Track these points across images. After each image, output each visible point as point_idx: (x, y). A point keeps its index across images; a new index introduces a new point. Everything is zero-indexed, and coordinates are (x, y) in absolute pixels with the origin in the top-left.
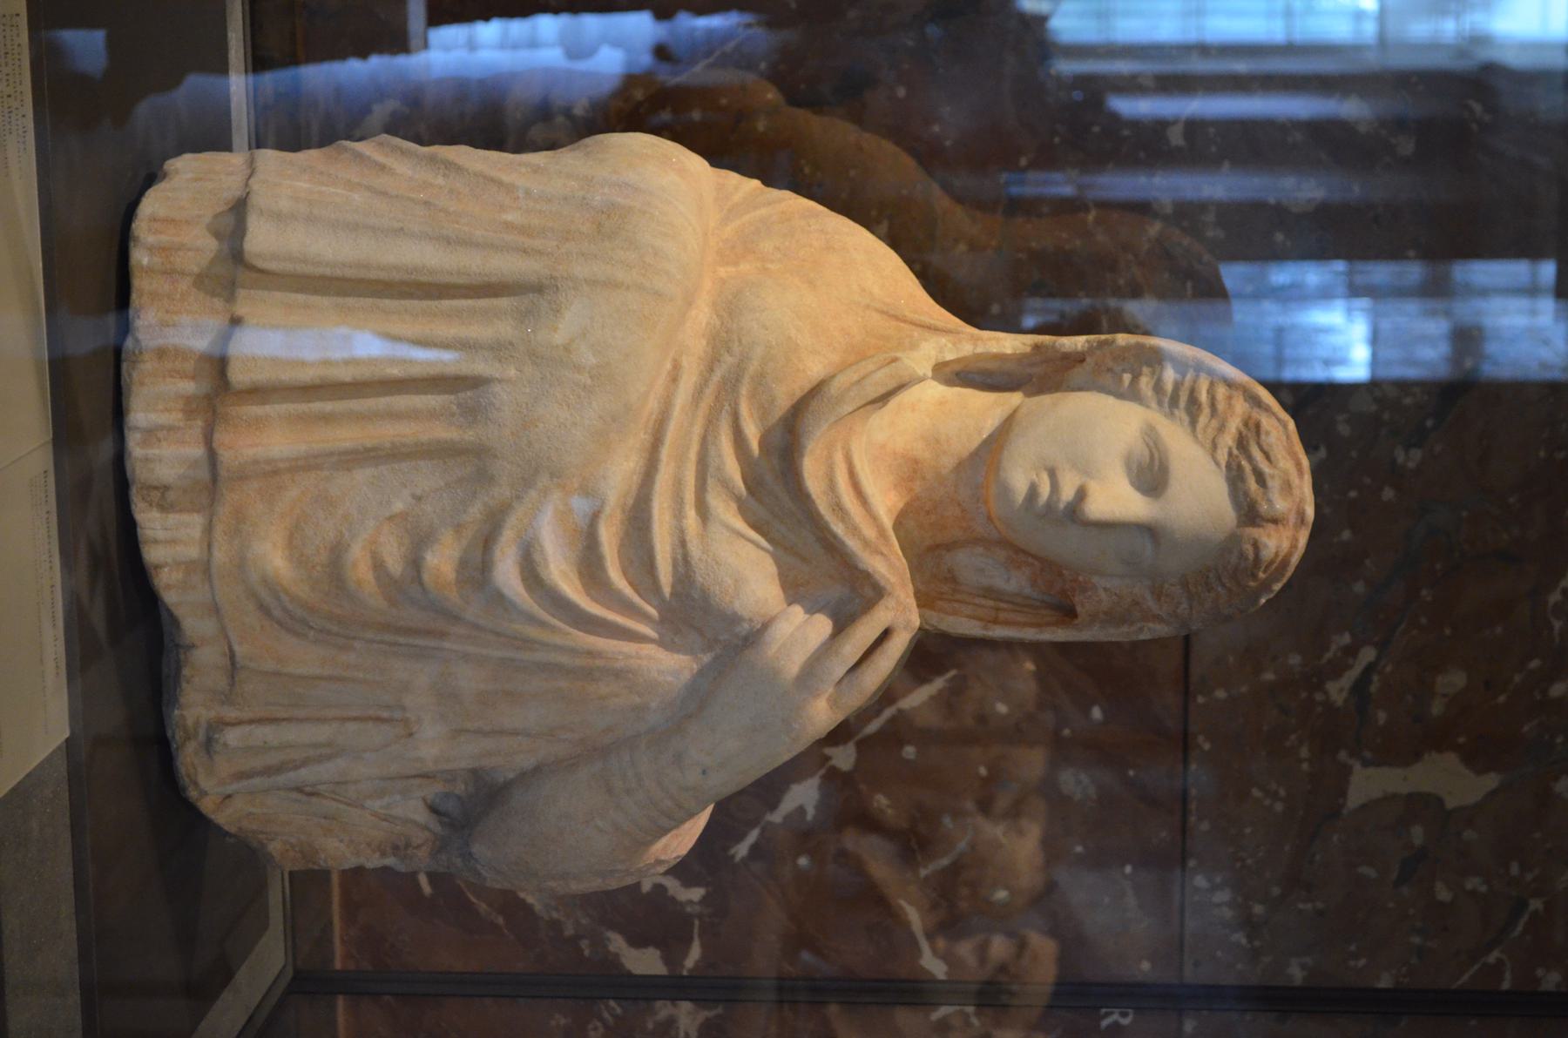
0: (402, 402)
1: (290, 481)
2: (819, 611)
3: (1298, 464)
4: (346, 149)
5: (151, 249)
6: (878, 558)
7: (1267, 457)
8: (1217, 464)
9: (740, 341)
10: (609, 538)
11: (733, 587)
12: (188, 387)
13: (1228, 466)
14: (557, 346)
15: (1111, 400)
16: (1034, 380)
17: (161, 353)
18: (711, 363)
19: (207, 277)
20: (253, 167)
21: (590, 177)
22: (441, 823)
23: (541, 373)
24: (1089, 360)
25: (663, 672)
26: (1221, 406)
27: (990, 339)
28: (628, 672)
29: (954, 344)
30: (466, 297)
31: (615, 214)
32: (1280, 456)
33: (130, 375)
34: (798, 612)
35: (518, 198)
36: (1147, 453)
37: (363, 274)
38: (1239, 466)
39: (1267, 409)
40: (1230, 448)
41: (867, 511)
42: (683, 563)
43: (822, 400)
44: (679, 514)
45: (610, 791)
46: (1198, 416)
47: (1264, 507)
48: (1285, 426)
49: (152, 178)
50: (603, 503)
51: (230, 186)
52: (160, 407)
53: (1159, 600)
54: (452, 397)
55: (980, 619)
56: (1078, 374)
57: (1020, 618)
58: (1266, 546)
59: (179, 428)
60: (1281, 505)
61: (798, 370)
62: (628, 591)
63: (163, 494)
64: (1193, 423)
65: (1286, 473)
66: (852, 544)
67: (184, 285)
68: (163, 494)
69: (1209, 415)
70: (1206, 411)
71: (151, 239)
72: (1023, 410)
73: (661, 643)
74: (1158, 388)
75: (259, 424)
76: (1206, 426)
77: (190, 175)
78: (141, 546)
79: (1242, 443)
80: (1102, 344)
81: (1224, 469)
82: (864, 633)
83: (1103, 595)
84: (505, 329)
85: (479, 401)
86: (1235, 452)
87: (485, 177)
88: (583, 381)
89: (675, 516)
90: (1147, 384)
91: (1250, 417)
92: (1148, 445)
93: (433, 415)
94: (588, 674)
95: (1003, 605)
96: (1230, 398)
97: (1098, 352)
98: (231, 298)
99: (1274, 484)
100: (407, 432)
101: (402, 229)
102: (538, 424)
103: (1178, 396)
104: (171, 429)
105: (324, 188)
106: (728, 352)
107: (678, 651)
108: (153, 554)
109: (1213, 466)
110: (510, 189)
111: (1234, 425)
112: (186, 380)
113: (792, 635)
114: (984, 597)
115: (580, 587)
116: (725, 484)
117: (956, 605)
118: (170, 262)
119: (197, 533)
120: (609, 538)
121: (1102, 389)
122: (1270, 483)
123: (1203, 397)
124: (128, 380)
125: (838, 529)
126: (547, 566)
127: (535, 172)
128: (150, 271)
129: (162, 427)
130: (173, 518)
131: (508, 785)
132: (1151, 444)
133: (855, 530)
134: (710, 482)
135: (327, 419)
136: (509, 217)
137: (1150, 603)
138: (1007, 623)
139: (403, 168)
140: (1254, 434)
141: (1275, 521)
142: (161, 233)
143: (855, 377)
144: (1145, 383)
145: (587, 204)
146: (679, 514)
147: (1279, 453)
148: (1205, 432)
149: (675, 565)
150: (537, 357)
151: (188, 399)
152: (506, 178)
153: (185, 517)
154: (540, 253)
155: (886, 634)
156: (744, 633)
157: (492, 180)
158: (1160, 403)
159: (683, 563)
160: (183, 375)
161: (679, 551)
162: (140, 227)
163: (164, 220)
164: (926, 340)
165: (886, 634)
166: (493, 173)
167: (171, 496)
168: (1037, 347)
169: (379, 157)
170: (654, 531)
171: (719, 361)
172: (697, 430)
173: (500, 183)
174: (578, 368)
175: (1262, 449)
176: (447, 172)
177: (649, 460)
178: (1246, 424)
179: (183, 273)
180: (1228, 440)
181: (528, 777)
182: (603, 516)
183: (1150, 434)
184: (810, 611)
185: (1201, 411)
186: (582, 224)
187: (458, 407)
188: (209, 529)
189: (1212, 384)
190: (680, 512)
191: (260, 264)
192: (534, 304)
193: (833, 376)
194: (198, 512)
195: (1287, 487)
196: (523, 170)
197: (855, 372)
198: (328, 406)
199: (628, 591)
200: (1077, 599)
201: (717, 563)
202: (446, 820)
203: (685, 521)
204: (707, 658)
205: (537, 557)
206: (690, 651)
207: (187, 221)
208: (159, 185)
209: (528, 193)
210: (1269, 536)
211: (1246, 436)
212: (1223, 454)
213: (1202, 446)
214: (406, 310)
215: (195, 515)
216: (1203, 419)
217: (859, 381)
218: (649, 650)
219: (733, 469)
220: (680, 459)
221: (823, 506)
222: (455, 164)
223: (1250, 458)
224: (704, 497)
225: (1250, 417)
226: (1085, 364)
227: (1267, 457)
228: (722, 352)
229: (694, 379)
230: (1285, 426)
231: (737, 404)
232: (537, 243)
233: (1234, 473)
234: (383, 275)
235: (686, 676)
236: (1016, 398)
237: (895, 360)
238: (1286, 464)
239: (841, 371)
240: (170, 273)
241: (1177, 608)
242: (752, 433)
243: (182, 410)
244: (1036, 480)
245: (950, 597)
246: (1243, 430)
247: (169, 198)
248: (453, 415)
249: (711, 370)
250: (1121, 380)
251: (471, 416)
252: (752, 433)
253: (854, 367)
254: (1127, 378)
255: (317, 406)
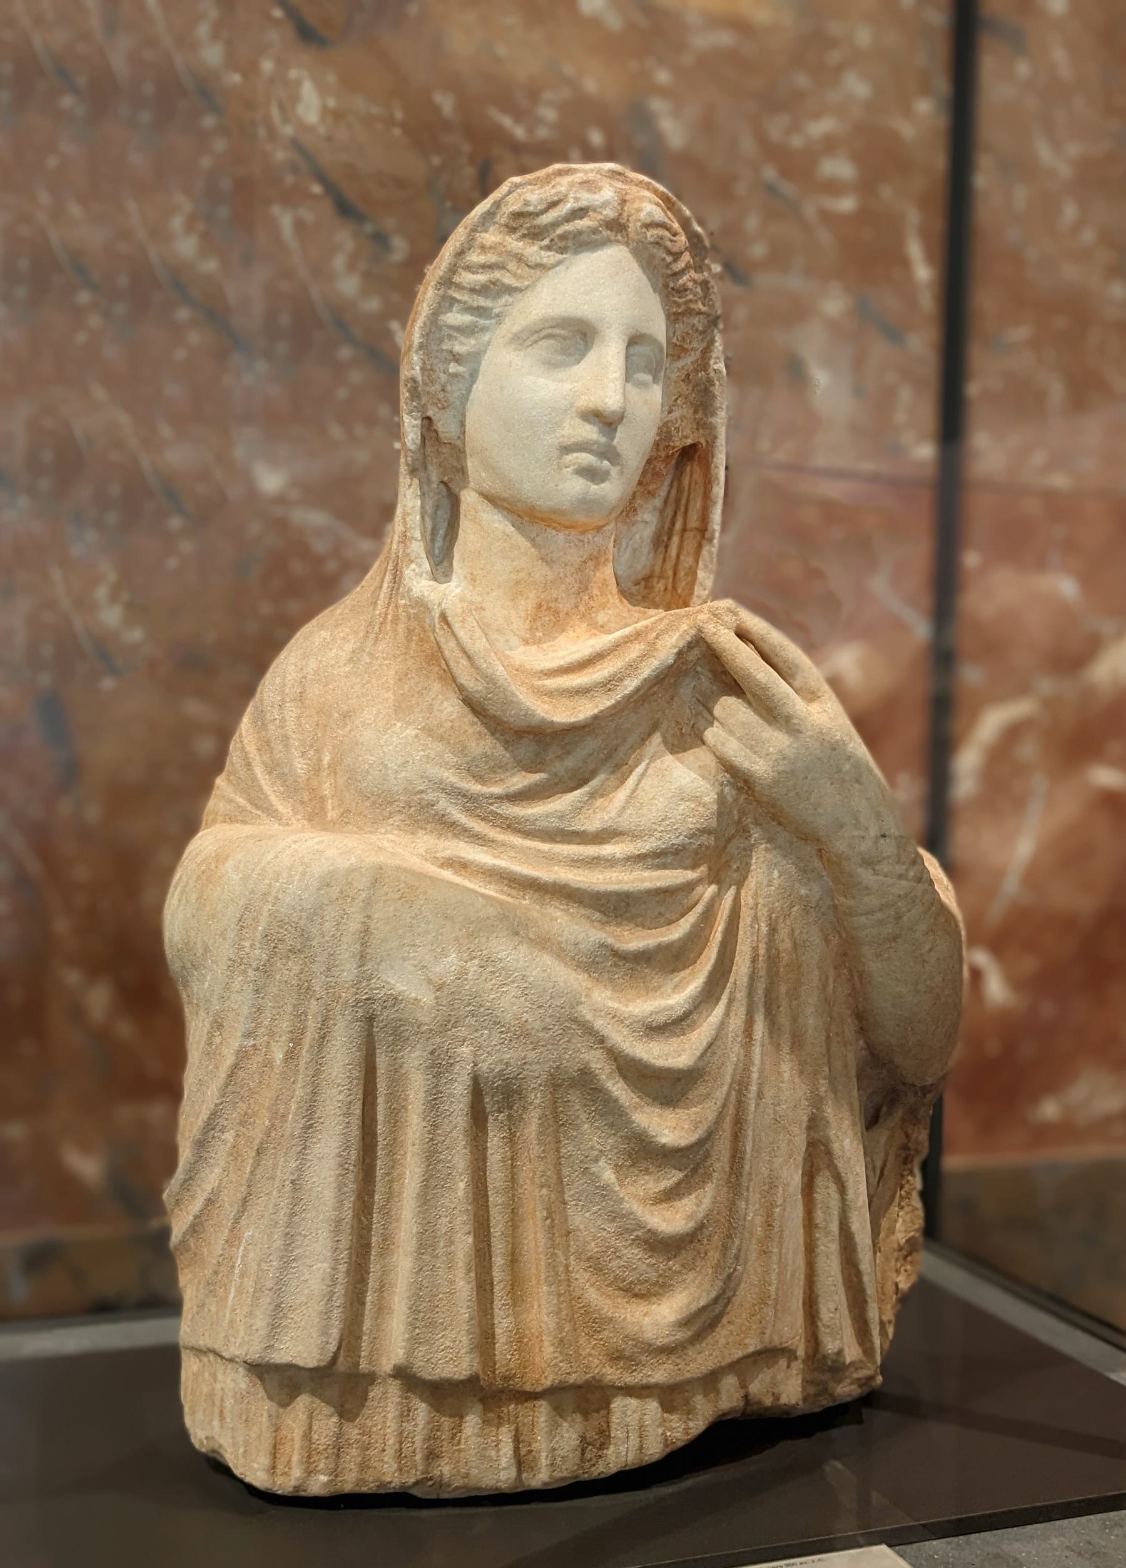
0: (496, 1176)
1: (580, 1301)
2: (710, 711)
3: (560, 173)
4: (183, 1242)
5: (310, 1472)
6: (659, 644)
7: (553, 205)
8: (559, 263)
9: (422, 792)
10: (635, 940)
11: (688, 803)
12: (472, 1422)
13: (562, 250)
14: (436, 998)
15: (478, 386)
16: (446, 479)
17: (432, 1455)
18: (447, 826)
19: (342, 1406)
20: (204, 1349)
21: (230, 963)
22: (889, 1114)
23: (467, 1017)
24: (430, 413)
25: (769, 881)
26: (491, 258)
27: (405, 523)
28: (770, 919)
29: (412, 562)
30: (374, 1104)
31: (278, 933)
32: (554, 191)
33: (456, 1488)
34: (712, 734)
35: (254, 1045)
36: (544, 343)
37: (346, 1227)
38: (563, 237)
39: (497, 205)
40: (541, 248)
41: (609, 654)
42: (660, 858)
43: (490, 699)
44: (610, 862)
45: (895, 938)
46: (504, 285)
47: (609, 213)
48: (517, 186)
49: (218, 1467)
50: (602, 945)
51: (236, 1381)
52: (493, 1453)
53: (686, 350)
54: (490, 1118)
55: (700, 547)
56: (446, 426)
57: (697, 504)
58: (649, 214)
59: (517, 1430)
60: (607, 193)
61: (452, 727)
62: (691, 919)
63: (589, 1444)
64: (511, 290)
65: (571, 185)
66: (647, 671)
67: (353, 1432)
68: (589, 1444)
69: (502, 272)
70: (497, 274)
71: (297, 1473)
72: (486, 487)
73: (740, 884)
74: (468, 331)
75: (520, 1339)
76: (515, 275)
77: (216, 1423)
78: (644, 1464)
79: (535, 235)
80: (415, 393)
81: (564, 256)
82: (744, 657)
83: (676, 414)
84: (414, 1060)
85: (497, 1088)
86: (546, 242)
87: (227, 1085)
88: (475, 968)
89: (612, 866)
90: (462, 344)
91: (506, 226)
92: (536, 342)
93: (511, 1140)
94: (773, 960)
95: (678, 526)
96: (483, 248)
97: (424, 400)
98: (371, 1378)
99: (586, 198)
100: (531, 1170)
101: (293, 1182)
102: (524, 1019)
103: (478, 308)
104: (517, 1440)
105: (237, 1271)
106: (433, 805)
107: (748, 864)
108: (654, 1450)
109: (561, 268)
110: (243, 1055)
111: (514, 244)
112: (464, 1425)
113: (740, 739)
114: (667, 547)
115: (687, 971)
116: (577, 810)
117: (682, 574)
118: (325, 1450)
119: (633, 1402)
120: (635, 940)
121: (465, 398)
122: (583, 203)
123: (482, 278)
124: (463, 1490)
125: (631, 685)
126: (672, 1007)
127: (220, 1026)
128: (335, 1473)
129: (517, 1450)
130: (617, 1432)
131: (870, 1047)
132: (535, 337)
133: (632, 667)
134: (576, 826)
135: (514, 1259)
136: (279, 1056)
137: (688, 361)
138: (705, 518)
139: (211, 1178)
140: (527, 220)
141: (624, 202)
142: (289, 1461)
143: (464, 662)
144: (462, 346)
145: (264, 965)
146: (610, 862)
147: (548, 192)
148: (521, 277)
149: (659, 867)
150: (449, 1021)
151: (486, 1422)
152: (229, 1061)
153: (615, 1419)
154: (325, 1019)
155: (743, 635)
156: (734, 792)
157: (231, 1075)
158: (484, 329)
159: (660, 858)
160: (457, 1429)
161: (650, 861)
162: (285, 1484)
163: (275, 1457)
164: (410, 590)
165: (743, 635)
166: (222, 1075)
167: (592, 1435)
168: (413, 472)
169: (196, 1207)
170: (631, 889)
171: (443, 816)
172: (518, 841)
173: (236, 1067)
174: (462, 974)
175: (546, 210)
176: (218, 1128)
177: (553, 894)
178: (513, 230)
179: (339, 1435)
180: (533, 251)
181: (863, 1020)
182: (617, 946)
183: (525, 339)
184: (711, 720)
185: (498, 280)
186: (289, 970)
187: (502, 1112)
188: (629, 1391)
189: (468, 268)
190: (608, 860)
191: (332, 1348)
192: (385, 1026)
193: (461, 688)
194: (609, 1403)
195: (589, 185)
196: (218, 1040)
197: (458, 663)
198: (498, 1261)
199: (691, 919)
200: (678, 443)
201: (663, 820)
202: (884, 1109)
203: (618, 855)
204: (756, 834)
205: (661, 1019)
206: (749, 850)
207: (276, 1431)
208: (227, 1459)
209: (248, 1035)
210: (639, 210)
211: (527, 229)
212: (548, 257)
213: (537, 280)
214: (388, 1174)
215: (612, 1406)
216: (508, 279)
217: (469, 657)
218: (746, 897)
219: (562, 803)
220: (550, 859)
221: (606, 702)
222: (209, 1118)
223: (555, 224)
224: (592, 833)
225: (506, 226)
226: (434, 418)
227: (553, 205)
228: (433, 812)
229: (462, 844)
230: (517, 186)
231: (491, 796)
232: (312, 1024)
233: (570, 243)
234: (348, 1204)
235: (774, 856)
236: (469, 498)
237: (444, 617)
238: (563, 184)
239: (454, 680)
240: (338, 1449)
241: (697, 330)
242: (520, 781)
243: (498, 1427)
244: (572, 467)
245: (671, 580)
246: (520, 234)
247: (245, 1452)
248: (510, 1117)
249: (453, 825)
250: (456, 375)
251: (512, 1096)
252: (520, 781)
253: (452, 664)
254: (453, 368)
255: (498, 1274)
